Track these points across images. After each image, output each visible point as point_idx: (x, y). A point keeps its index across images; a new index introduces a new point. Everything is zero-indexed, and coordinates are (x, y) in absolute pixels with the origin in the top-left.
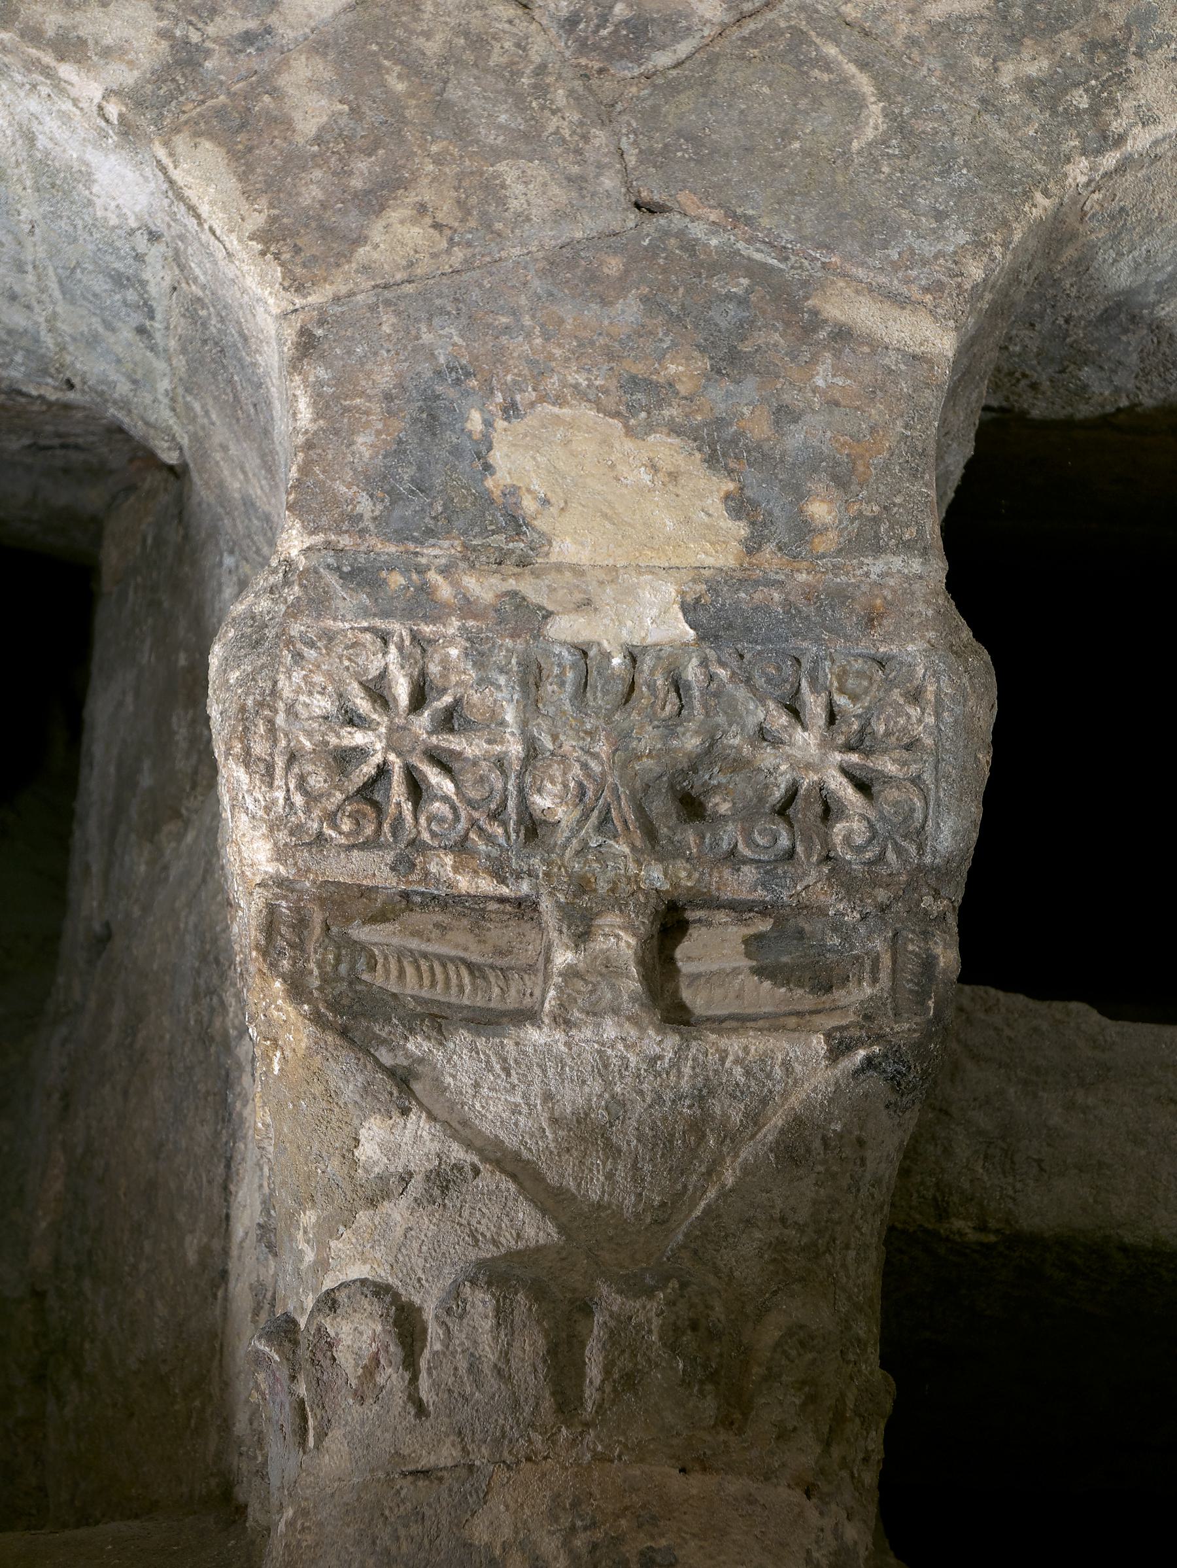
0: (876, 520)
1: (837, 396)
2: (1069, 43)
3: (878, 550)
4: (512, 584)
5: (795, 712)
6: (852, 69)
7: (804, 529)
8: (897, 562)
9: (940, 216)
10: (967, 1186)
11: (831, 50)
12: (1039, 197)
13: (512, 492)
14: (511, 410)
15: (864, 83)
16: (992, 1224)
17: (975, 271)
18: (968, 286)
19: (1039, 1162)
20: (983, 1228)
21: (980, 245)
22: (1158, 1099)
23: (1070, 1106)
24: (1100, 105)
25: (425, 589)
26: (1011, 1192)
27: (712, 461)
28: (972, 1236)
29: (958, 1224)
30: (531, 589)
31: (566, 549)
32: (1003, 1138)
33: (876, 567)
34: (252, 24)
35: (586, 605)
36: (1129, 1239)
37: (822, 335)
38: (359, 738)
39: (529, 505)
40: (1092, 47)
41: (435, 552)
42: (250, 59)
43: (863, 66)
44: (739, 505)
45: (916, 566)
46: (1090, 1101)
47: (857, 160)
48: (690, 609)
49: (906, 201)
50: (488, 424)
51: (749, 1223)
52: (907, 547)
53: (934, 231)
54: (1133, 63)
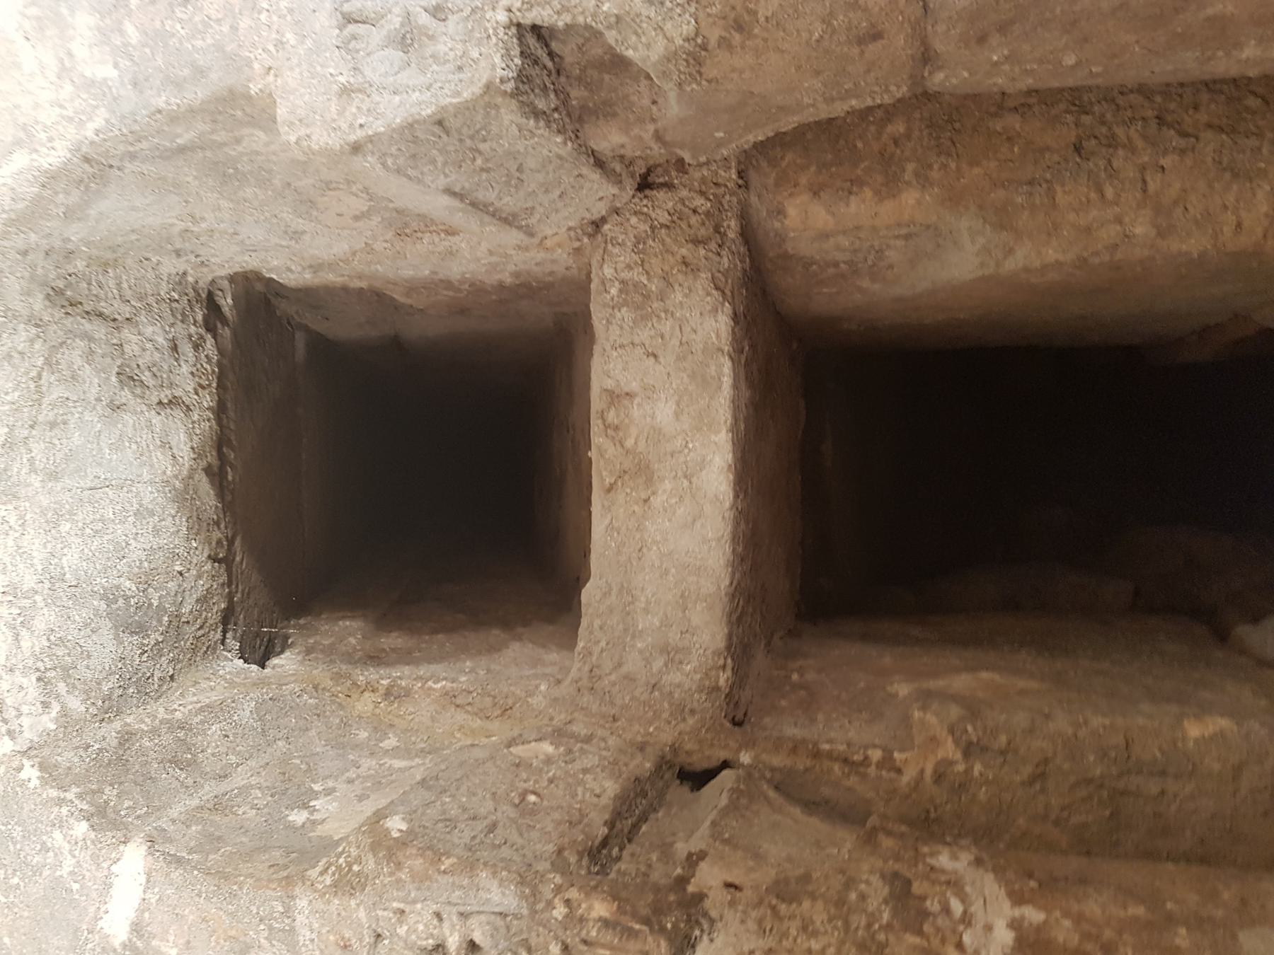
0: (271, 928)
1: (182, 941)
3: (293, 930)
8: (300, 919)
9: (45, 849)
10: (698, 676)
12: (23, 775)
16: (721, 662)
17: (81, 828)
18: (92, 835)
19: (682, 633)
20: (724, 667)
21: (60, 824)
22: (640, 559)
23: (646, 611)
26: (702, 651)
28: (729, 673)
29: (722, 682)
32: (669, 653)
33: (304, 935)
36: (727, 582)
37: (139, 944)
45: (302, 903)
46: (643, 599)
47: (11, 899)
49: (37, 871)
52: (288, 912)
53: (56, 855)
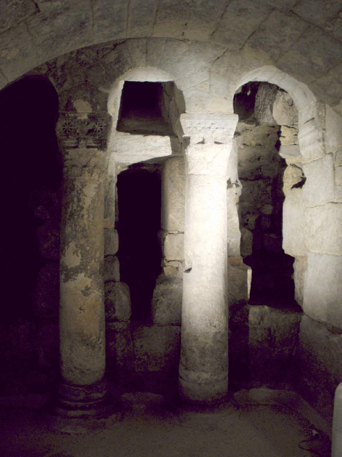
2: (120, 64)
4: (75, 115)
5: (96, 124)
6: (103, 67)
7: (97, 109)
11: (101, 65)
13: (75, 107)
14: (75, 100)
15: (104, 68)
24: (123, 70)
25: (68, 115)
27: (91, 104)
30: (76, 115)
31: (78, 111)
34: (54, 66)
35: (80, 116)
38: (64, 127)
39: (76, 108)
40: (122, 64)
41: (69, 112)
42: (55, 69)
43: (104, 66)
44: (92, 107)
48: (88, 116)
50: (73, 101)
51: (92, 162)
54: (125, 66)
